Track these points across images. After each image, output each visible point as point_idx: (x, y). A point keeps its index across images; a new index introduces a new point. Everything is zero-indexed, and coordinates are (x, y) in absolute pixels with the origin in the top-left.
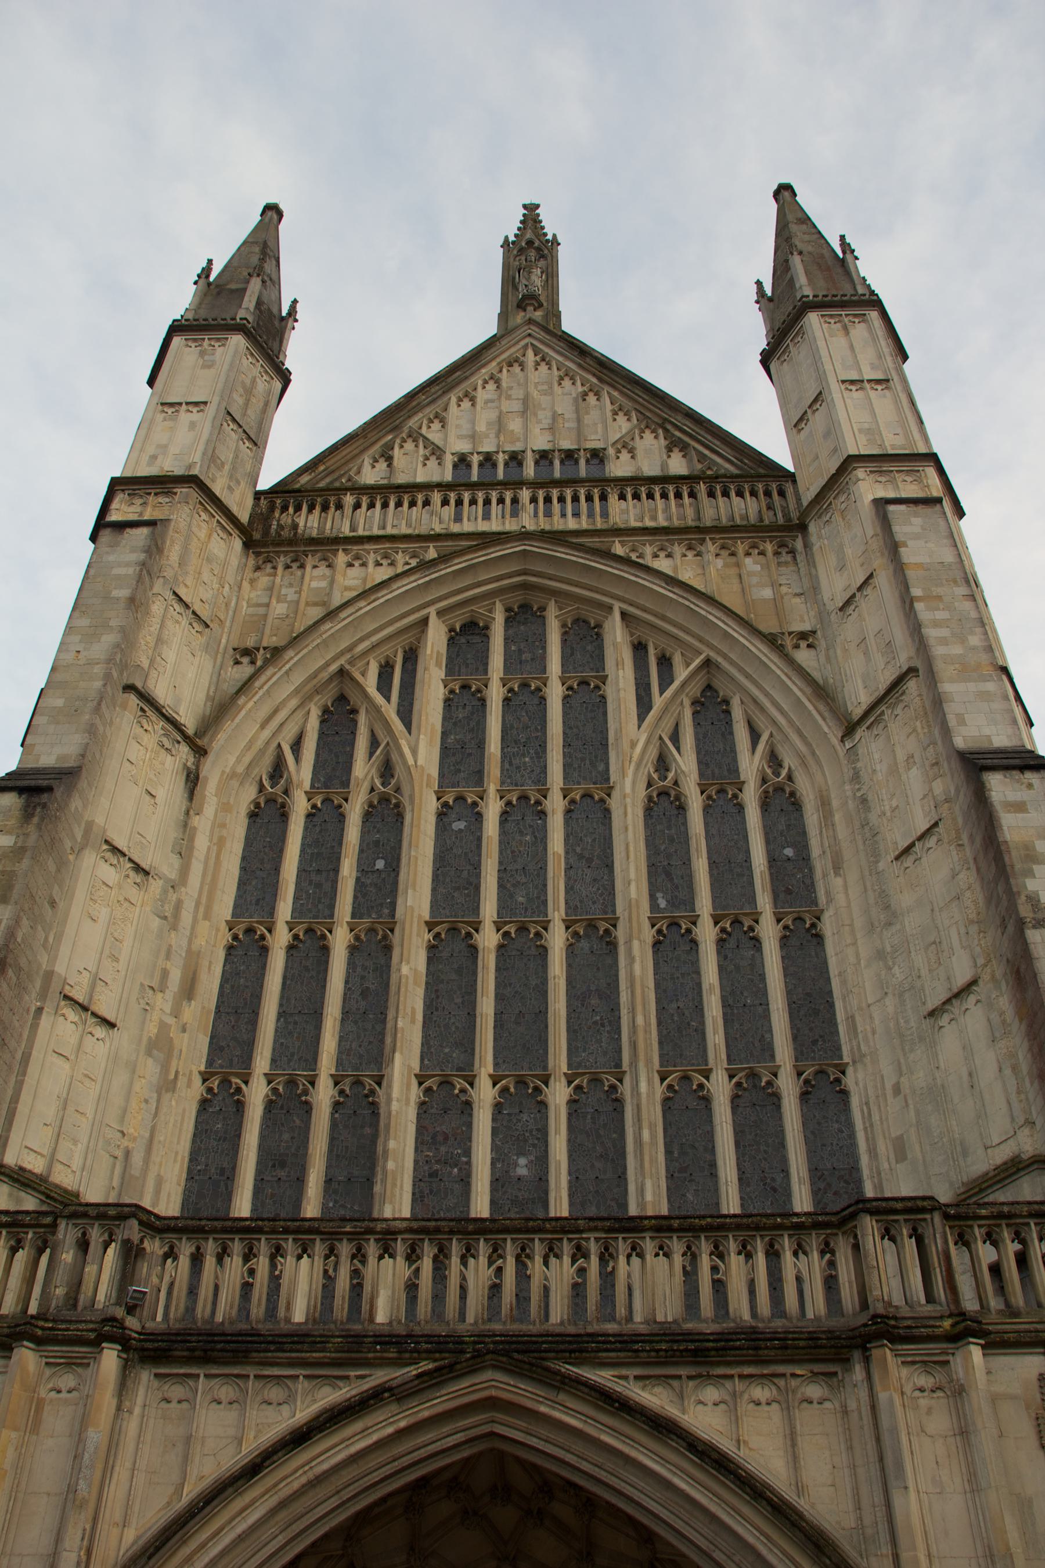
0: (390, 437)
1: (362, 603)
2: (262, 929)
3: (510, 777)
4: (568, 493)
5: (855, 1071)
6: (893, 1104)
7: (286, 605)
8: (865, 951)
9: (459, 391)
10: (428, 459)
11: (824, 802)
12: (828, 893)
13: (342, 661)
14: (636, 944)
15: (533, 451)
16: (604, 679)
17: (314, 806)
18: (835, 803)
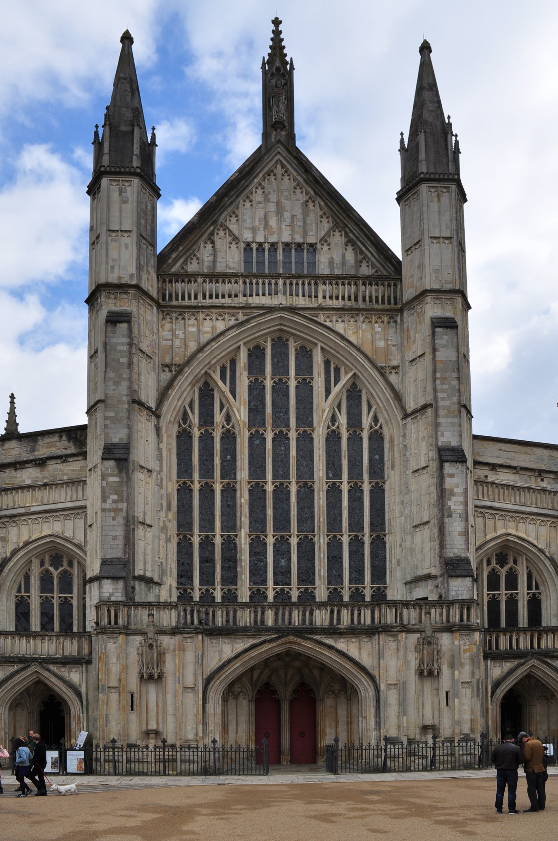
0: (212, 228)
1: (213, 343)
2: (189, 483)
3: (275, 422)
4: (300, 282)
6: (399, 550)
7: (179, 340)
8: (398, 499)
10: (231, 243)
11: (392, 441)
12: (388, 475)
13: (206, 369)
14: (321, 493)
15: (282, 243)
16: (312, 379)
17: (201, 433)
18: (396, 443)
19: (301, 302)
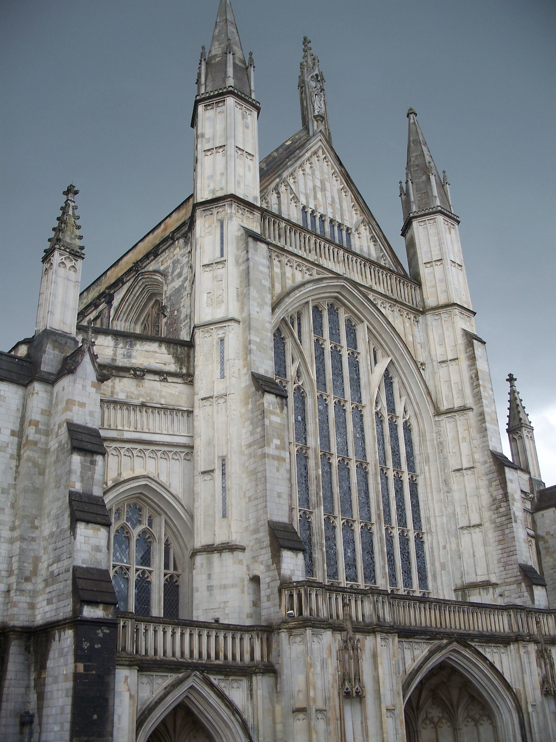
1: (296, 292)
5: (427, 536)
6: (442, 552)
9: (299, 163)
11: (422, 435)
12: (421, 470)
19: (357, 278)
